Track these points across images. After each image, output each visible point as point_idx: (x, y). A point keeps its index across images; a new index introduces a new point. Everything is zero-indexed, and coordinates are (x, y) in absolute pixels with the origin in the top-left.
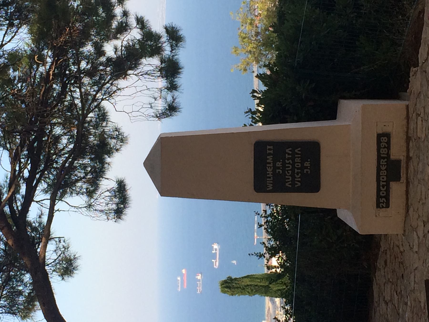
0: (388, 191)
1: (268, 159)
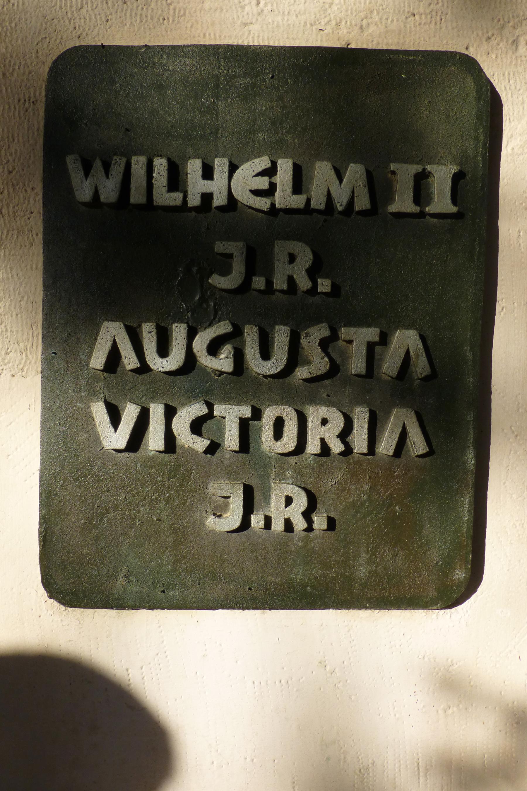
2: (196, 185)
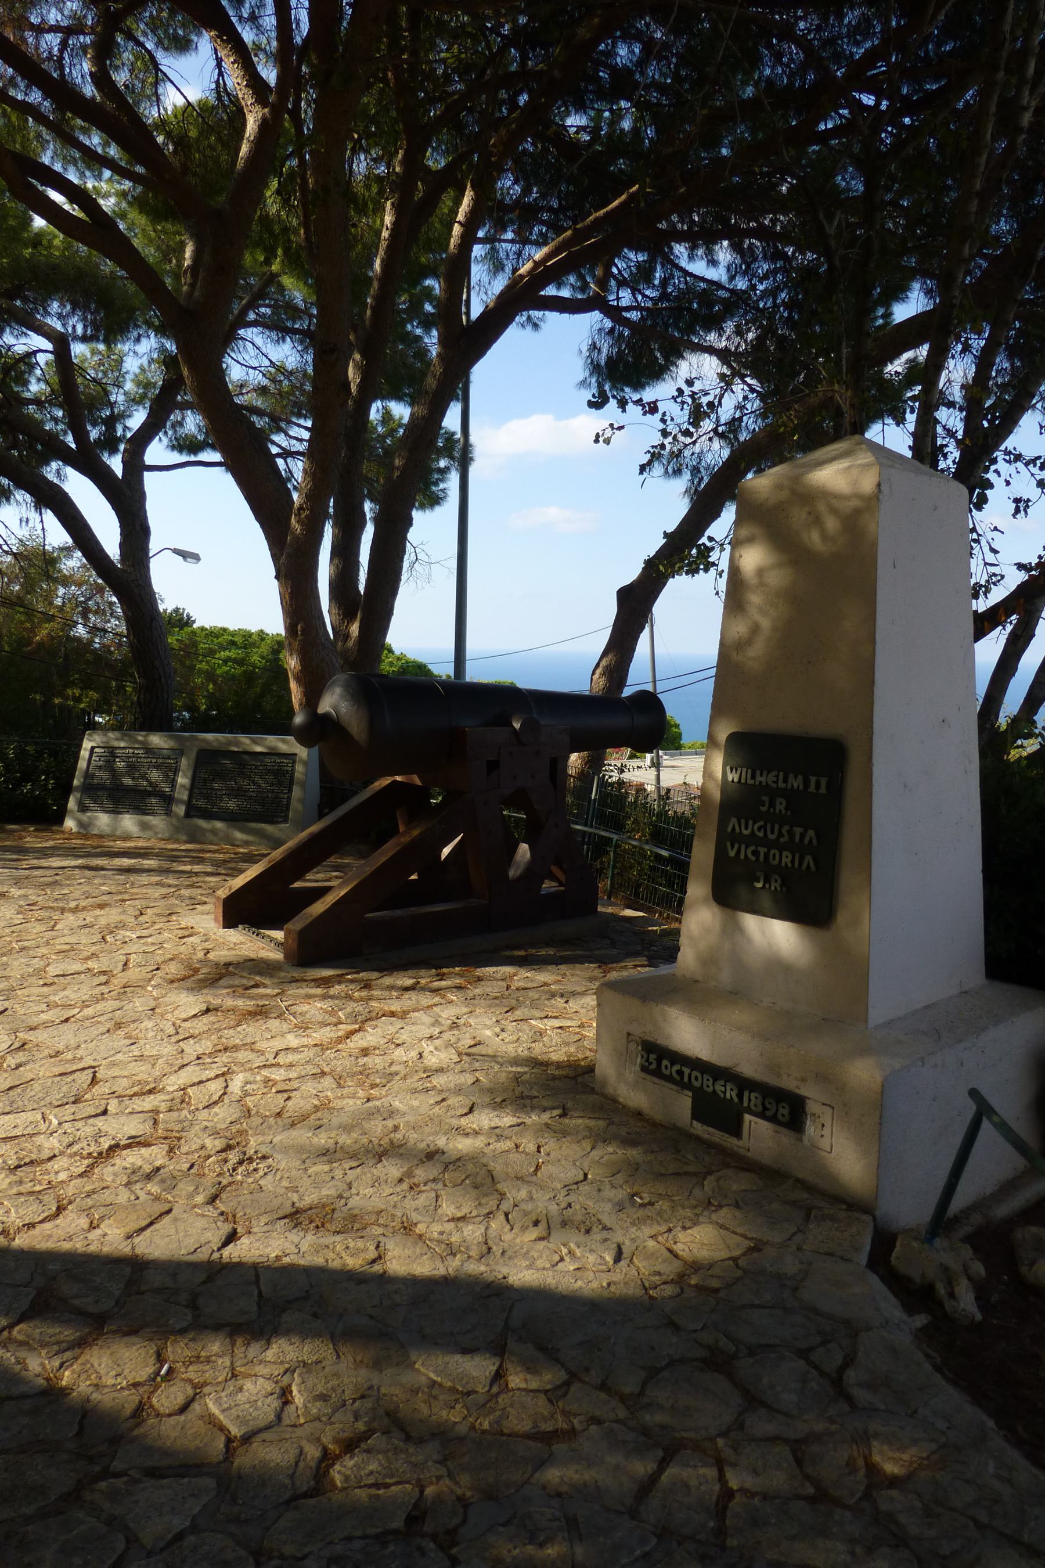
0: (669, 1079)
1: (796, 777)
2: (759, 779)
